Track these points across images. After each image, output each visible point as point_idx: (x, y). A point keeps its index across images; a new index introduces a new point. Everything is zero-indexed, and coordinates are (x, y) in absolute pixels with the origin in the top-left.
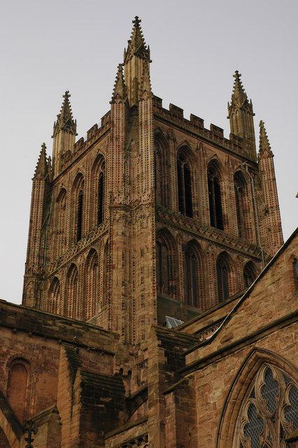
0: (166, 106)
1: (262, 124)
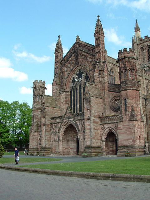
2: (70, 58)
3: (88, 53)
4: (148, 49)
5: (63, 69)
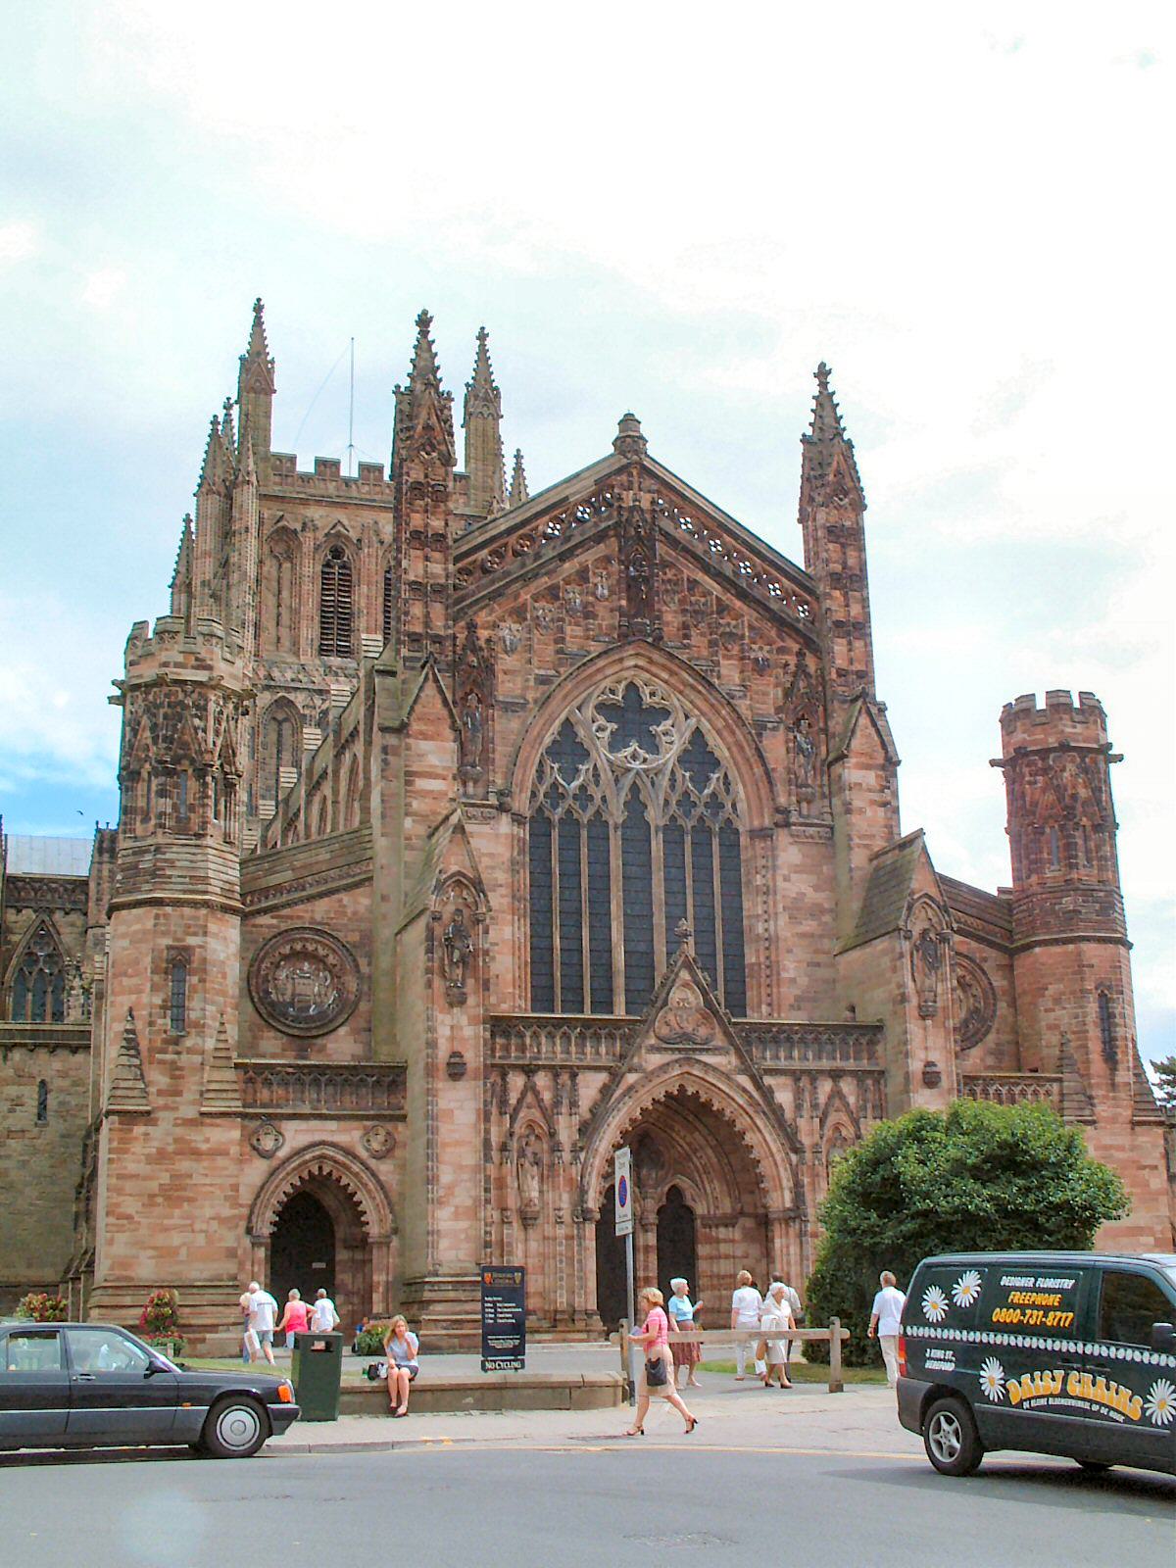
2: (563, 557)
3: (742, 595)
4: (328, 565)
5: (483, 617)
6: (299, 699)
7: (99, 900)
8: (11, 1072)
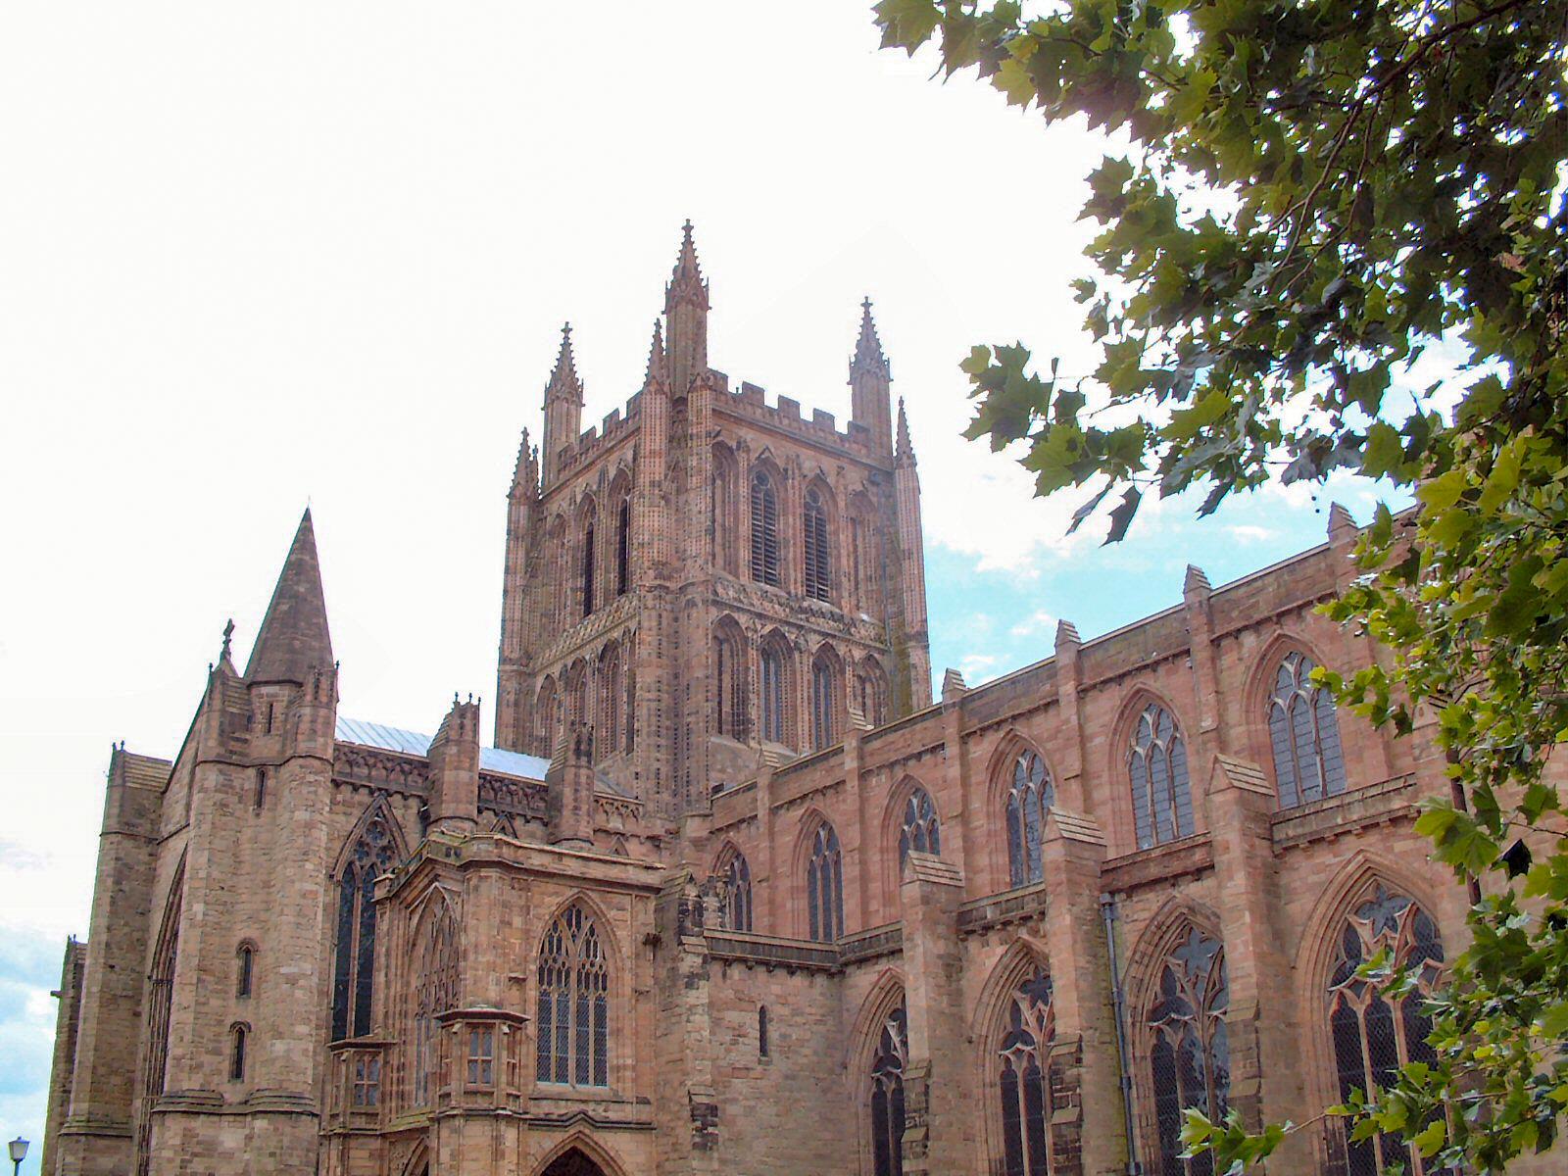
0: (733, 386)
1: (901, 402)
6: (743, 620)
7: (576, 808)
8: (730, 994)
